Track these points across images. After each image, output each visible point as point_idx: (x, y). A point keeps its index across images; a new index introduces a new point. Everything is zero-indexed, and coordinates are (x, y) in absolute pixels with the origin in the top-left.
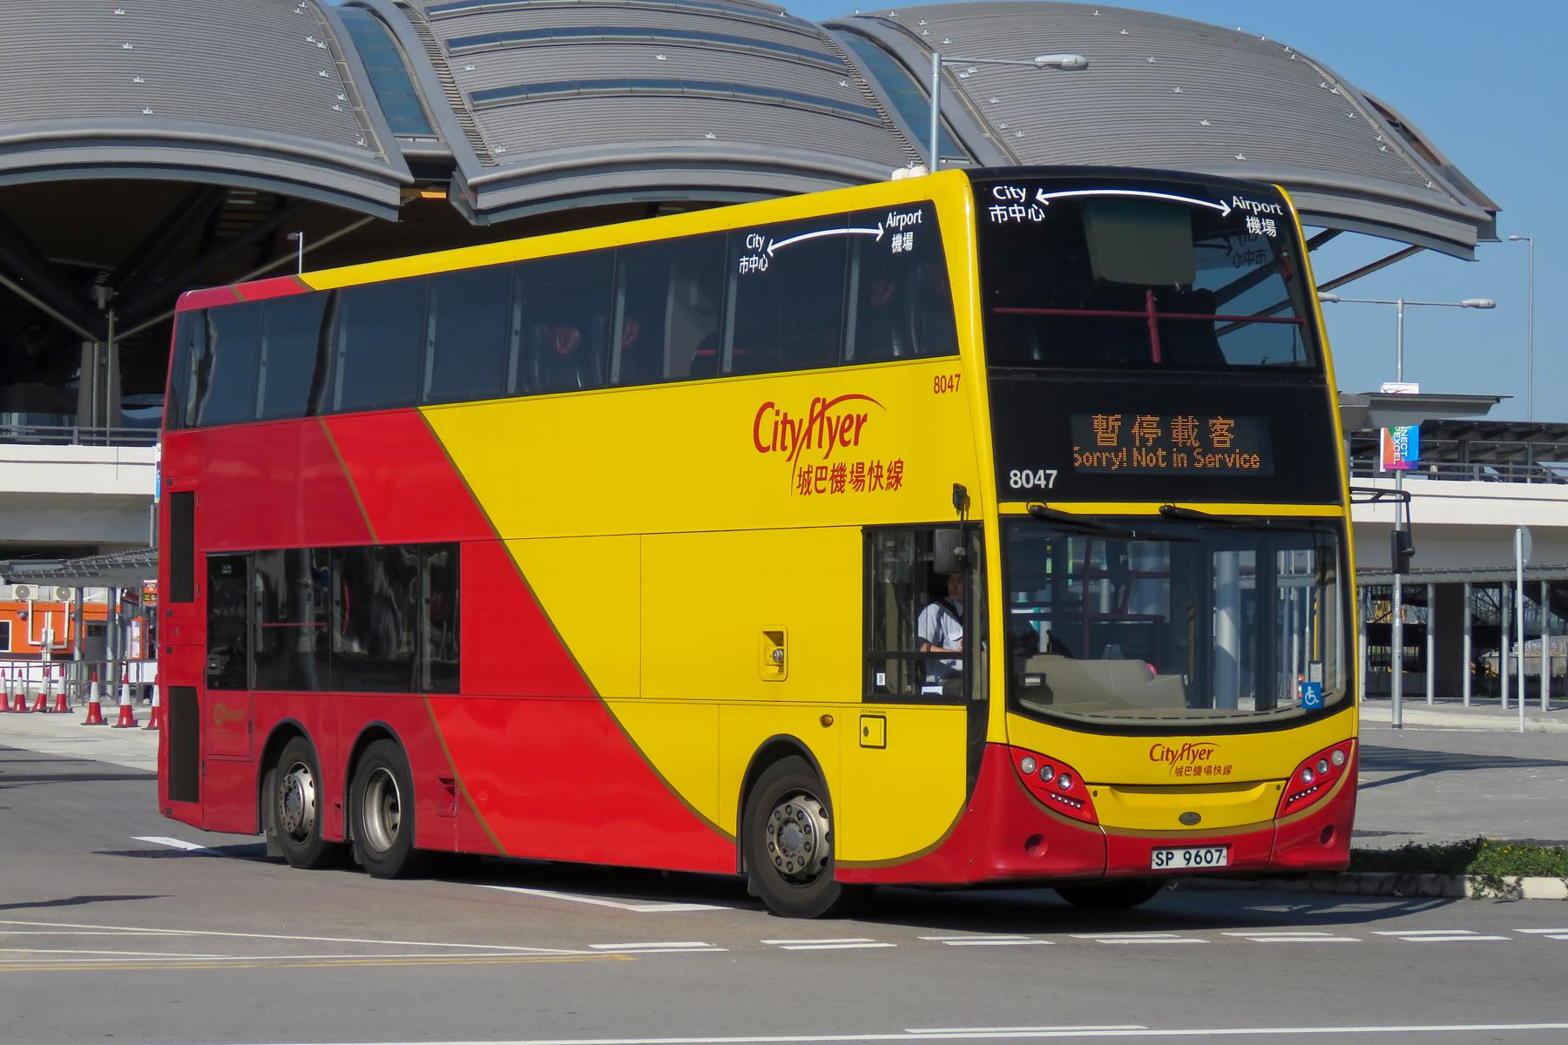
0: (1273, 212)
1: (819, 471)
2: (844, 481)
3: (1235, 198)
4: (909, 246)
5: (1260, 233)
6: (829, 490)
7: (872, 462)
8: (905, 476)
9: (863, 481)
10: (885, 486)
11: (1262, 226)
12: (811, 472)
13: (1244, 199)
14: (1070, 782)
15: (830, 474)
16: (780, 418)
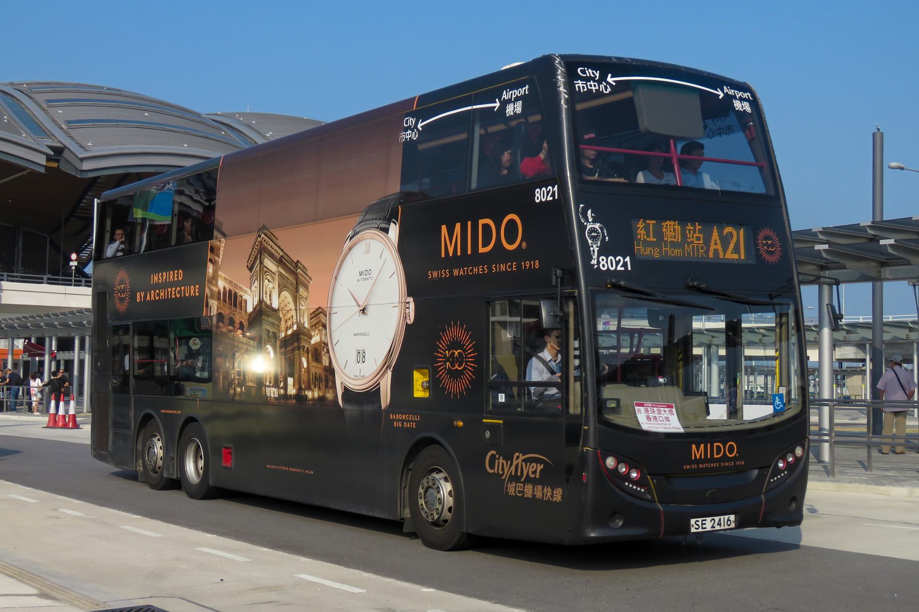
0: (747, 98)
3: (725, 87)
4: (519, 110)
5: (742, 110)
11: (742, 105)
13: (731, 89)
14: (638, 474)
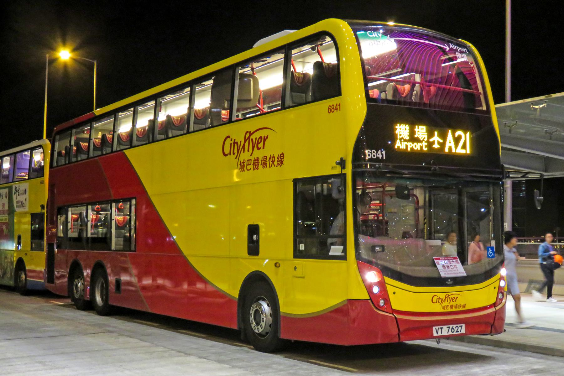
1: (248, 161)
2: (259, 165)
6: (252, 169)
7: (270, 155)
8: (285, 160)
9: (267, 164)
10: (276, 166)
12: (245, 162)
15: (252, 162)
16: (233, 141)
